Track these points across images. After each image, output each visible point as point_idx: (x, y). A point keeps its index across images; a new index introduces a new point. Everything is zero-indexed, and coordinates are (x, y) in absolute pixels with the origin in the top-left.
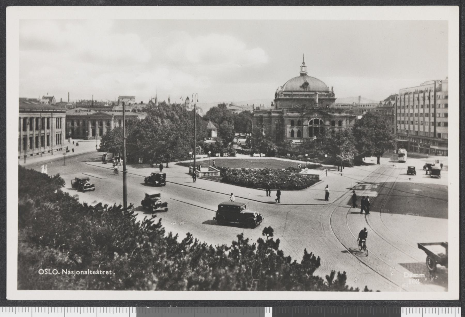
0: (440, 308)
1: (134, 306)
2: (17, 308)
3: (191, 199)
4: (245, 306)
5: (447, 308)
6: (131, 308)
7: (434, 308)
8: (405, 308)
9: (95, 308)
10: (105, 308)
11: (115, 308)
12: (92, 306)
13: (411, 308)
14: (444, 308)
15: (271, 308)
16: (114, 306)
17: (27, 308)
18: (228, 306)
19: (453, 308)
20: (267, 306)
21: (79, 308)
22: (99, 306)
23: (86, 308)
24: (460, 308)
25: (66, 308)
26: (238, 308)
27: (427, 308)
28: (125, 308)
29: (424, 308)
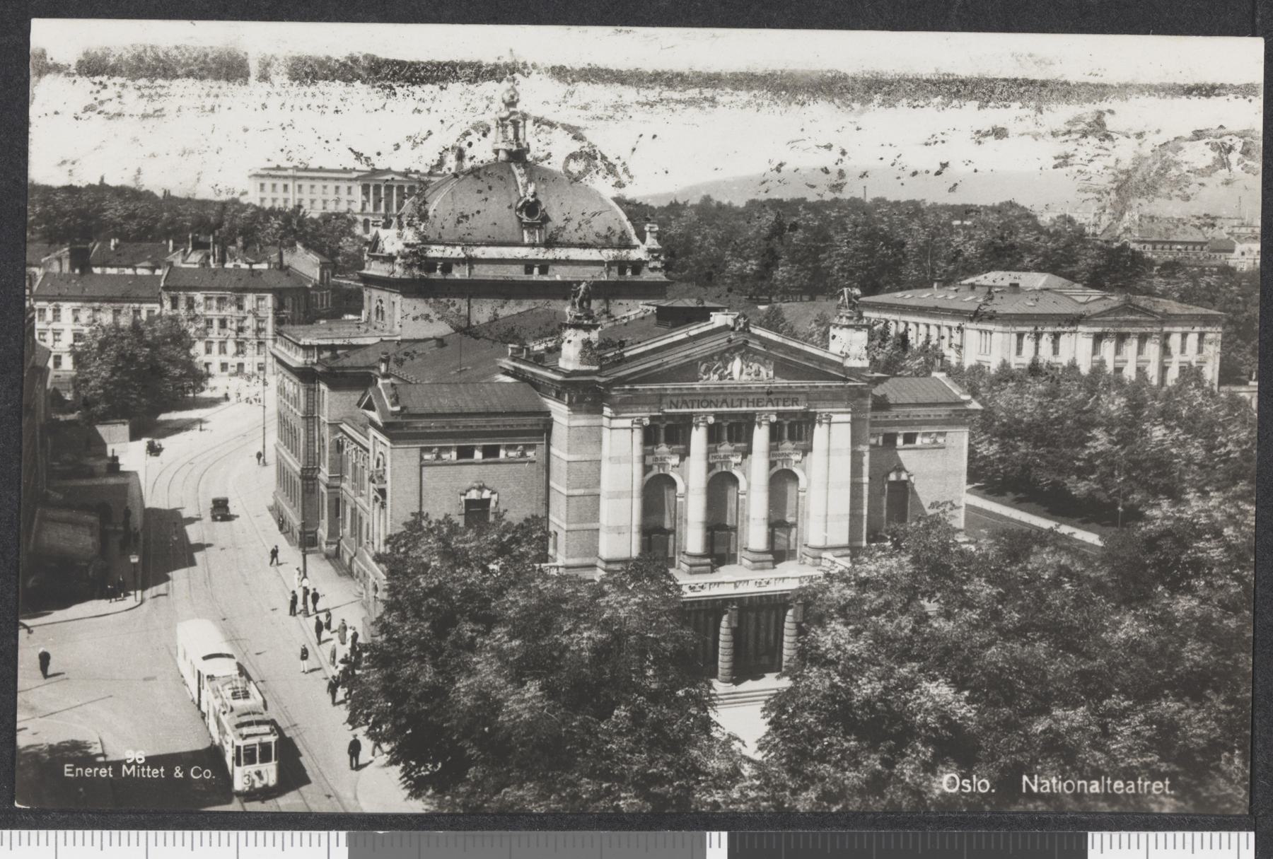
0: (1198, 834)
1: (342, 829)
2: (15, 833)
3: (1012, 520)
4: (651, 829)
5: (1216, 835)
6: (333, 833)
7: (1179, 834)
8: (1097, 835)
9: (233, 833)
10: (260, 833)
11: (288, 833)
12: (225, 829)
13: (1116, 835)
14: (1207, 834)
15: (724, 835)
16: (285, 829)
17: (43, 833)
18: (605, 829)
19: (1234, 835)
20: (713, 830)
21: (188, 833)
22: (242, 829)
23: (206, 833)
24: (1252, 834)
25: (152, 833)
26: (633, 833)
27: (1161, 834)
28: (315, 834)
29: (1152, 835)
